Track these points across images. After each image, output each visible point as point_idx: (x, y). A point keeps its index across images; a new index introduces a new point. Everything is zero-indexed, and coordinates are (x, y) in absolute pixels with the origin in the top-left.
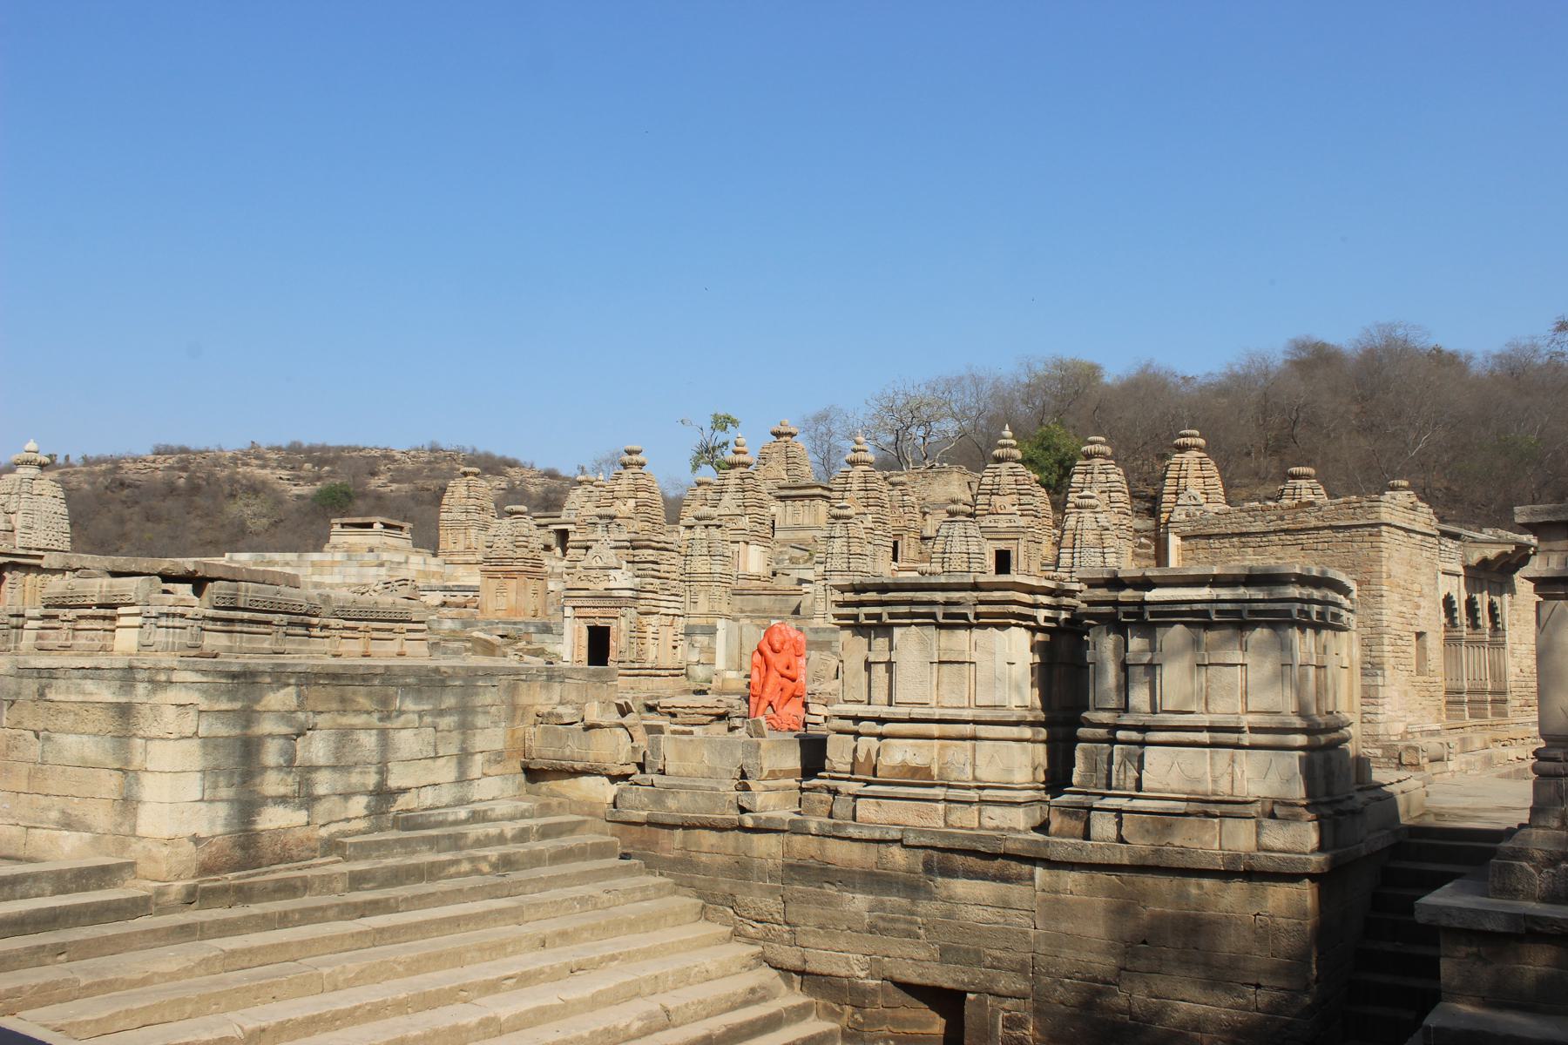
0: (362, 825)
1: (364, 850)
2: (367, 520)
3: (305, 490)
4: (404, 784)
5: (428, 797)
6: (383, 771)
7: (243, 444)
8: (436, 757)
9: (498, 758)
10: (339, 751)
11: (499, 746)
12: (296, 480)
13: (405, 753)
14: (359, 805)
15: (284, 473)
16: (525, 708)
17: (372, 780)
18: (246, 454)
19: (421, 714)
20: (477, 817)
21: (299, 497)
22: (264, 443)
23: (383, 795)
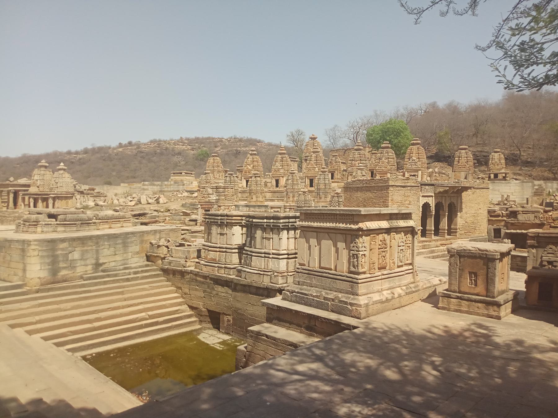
0: (91, 272)
1: (89, 278)
2: (180, 172)
3: (195, 152)
4: (104, 261)
5: (113, 264)
6: (97, 259)
7: (178, 138)
8: (115, 255)
9: (138, 253)
10: (82, 255)
11: (138, 250)
12: (193, 149)
13: (105, 254)
14: (90, 268)
15: (189, 147)
16: (146, 241)
17: (94, 261)
18: (178, 141)
19: (109, 245)
20: (125, 269)
21: (194, 155)
22: (184, 137)
23: (97, 265)
